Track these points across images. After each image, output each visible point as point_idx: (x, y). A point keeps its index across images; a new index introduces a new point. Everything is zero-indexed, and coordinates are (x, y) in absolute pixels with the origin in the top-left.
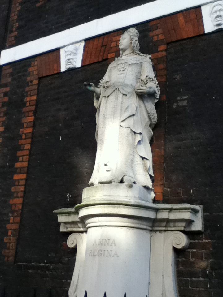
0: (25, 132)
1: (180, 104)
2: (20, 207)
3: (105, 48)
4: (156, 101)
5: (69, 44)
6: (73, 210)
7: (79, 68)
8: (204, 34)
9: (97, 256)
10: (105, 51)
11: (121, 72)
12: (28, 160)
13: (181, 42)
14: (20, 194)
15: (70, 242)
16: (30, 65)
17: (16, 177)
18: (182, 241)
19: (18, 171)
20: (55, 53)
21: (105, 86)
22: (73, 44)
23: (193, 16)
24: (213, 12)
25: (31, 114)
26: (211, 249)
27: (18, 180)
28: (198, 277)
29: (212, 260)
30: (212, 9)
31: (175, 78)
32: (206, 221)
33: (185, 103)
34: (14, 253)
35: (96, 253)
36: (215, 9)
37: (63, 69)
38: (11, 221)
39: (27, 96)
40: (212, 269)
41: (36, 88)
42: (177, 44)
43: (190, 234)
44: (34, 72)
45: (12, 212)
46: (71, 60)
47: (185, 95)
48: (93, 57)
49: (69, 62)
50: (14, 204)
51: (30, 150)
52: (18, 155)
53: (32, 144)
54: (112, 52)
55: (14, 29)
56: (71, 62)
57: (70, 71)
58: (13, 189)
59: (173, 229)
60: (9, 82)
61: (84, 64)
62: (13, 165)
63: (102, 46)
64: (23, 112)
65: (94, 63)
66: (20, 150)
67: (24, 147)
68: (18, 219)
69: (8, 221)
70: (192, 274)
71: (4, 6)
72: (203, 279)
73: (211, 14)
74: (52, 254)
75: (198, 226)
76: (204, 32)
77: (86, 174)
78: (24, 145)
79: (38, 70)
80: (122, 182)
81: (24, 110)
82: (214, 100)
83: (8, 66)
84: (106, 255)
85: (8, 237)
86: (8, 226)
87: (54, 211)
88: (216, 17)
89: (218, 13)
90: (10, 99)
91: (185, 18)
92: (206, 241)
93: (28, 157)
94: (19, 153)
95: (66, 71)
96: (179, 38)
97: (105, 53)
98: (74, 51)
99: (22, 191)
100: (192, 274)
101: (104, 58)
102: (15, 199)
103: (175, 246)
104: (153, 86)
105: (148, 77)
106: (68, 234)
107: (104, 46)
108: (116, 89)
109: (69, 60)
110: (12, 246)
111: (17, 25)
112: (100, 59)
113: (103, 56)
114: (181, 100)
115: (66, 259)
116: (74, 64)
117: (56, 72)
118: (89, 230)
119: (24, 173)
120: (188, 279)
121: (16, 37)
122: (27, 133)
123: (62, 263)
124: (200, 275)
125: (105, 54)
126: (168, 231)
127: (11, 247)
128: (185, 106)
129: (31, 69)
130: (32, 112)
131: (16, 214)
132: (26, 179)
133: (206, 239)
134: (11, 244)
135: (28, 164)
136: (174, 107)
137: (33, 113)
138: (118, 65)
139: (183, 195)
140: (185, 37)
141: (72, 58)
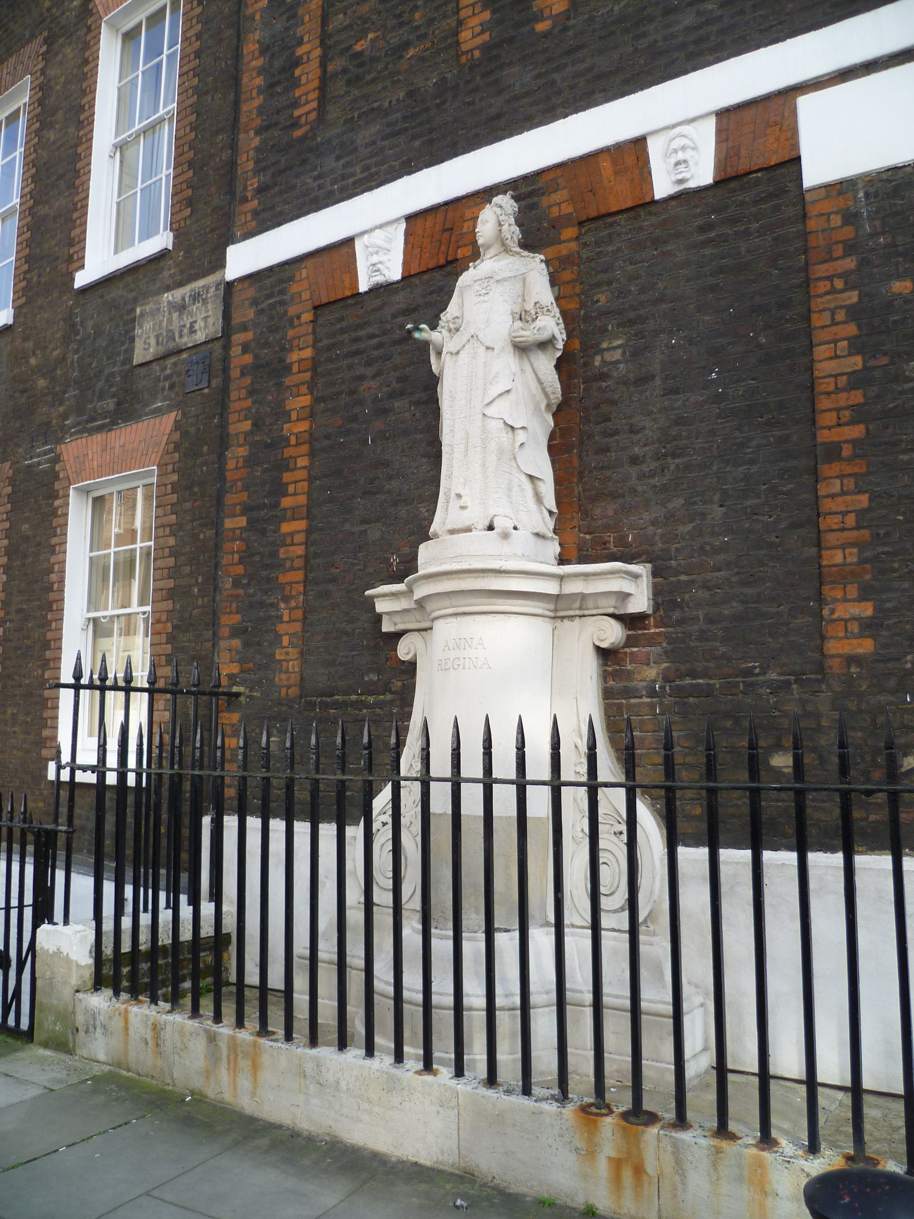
0: (295, 431)
1: (608, 357)
2: (301, 588)
4: (559, 354)
5: (372, 227)
6: (401, 587)
7: (398, 282)
8: (654, 202)
9: (451, 669)
11: (482, 298)
12: (306, 490)
13: (610, 220)
14: (299, 563)
15: (404, 651)
16: (291, 279)
17: (286, 528)
18: (612, 633)
19: (289, 514)
20: (344, 250)
21: (452, 326)
22: (381, 227)
23: (630, 160)
24: (670, 151)
25: (304, 389)
26: (664, 645)
27: (292, 534)
28: (641, 697)
29: (666, 665)
31: (598, 301)
32: (657, 592)
33: (617, 355)
34: (298, 678)
36: (675, 144)
37: (363, 287)
38: (286, 618)
40: (666, 679)
41: (310, 330)
42: (600, 223)
44: (303, 293)
45: (286, 599)
46: (379, 266)
49: (376, 271)
50: (287, 583)
51: (309, 468)
52: (285, 480)
53: (312, 454)
54: (465, 245)
55: (249, 195)
56: (379, 270)
57: (377, 290)
58: (282, 553)
60: (251, 320)
61: (407, 274)
62: (277, 504)
63: (445, 230)
64: (288, 387)
65: (428, 270)
66: (288, 470)
67: (296, 463)
68: (299, 614)
69: (280, 618)
70: (628, 693)
71: (221, 137)
72: (648, 700)
73: (666, 156)
74: (371, 676)
77: (426, 514)
78: (295, 458)
79: (310, 289)
80: (491, 528)
81: (289, 381)
82: (673, 346)
83: (246, 284)
85: (284, 650)
86: (281, 628)
87: (367, 593)
88: (678, 164)
89: (681, 156)
90: (256, 357)
91: (615, 163)
92: (657, 630)
93: (305, 483)
94: (287, 477)
95: (371, 290)
96: (603, 211)
98: (386, 245)
99: (300, 557)
100: (628, 693)
101: (450, 259)
102: (290, 573)
104: (551, 325)
105: (538, 305)
106: (397, 636)
107: (448, 229)
108: (472, 336)
109: (374, 265)
110: (294, 666)
111: (253, 183)
112: (442, 261)
114: (608, 349)
115: (399, 684)
116: (385, 272)
117: (348, 293)
118: (439, 625)
119: (302, 519)
120: (624, 701)
121: (256, 213)
122: (300, 432)
123: (391, 692)
124: (644, 693)
126: (584, 616)
127: (291, 670)
128: (618, 362)
129: (294, 288)
130: (306, 386)
131: (293, 603)
132: (308, 531)
133: (656, 626)
134: (291, 663)
135: (309, 499)
136: (597, 364)
137: (308, 388)
139: (615, 547)
140: (614, 209)
141: (382, 261)
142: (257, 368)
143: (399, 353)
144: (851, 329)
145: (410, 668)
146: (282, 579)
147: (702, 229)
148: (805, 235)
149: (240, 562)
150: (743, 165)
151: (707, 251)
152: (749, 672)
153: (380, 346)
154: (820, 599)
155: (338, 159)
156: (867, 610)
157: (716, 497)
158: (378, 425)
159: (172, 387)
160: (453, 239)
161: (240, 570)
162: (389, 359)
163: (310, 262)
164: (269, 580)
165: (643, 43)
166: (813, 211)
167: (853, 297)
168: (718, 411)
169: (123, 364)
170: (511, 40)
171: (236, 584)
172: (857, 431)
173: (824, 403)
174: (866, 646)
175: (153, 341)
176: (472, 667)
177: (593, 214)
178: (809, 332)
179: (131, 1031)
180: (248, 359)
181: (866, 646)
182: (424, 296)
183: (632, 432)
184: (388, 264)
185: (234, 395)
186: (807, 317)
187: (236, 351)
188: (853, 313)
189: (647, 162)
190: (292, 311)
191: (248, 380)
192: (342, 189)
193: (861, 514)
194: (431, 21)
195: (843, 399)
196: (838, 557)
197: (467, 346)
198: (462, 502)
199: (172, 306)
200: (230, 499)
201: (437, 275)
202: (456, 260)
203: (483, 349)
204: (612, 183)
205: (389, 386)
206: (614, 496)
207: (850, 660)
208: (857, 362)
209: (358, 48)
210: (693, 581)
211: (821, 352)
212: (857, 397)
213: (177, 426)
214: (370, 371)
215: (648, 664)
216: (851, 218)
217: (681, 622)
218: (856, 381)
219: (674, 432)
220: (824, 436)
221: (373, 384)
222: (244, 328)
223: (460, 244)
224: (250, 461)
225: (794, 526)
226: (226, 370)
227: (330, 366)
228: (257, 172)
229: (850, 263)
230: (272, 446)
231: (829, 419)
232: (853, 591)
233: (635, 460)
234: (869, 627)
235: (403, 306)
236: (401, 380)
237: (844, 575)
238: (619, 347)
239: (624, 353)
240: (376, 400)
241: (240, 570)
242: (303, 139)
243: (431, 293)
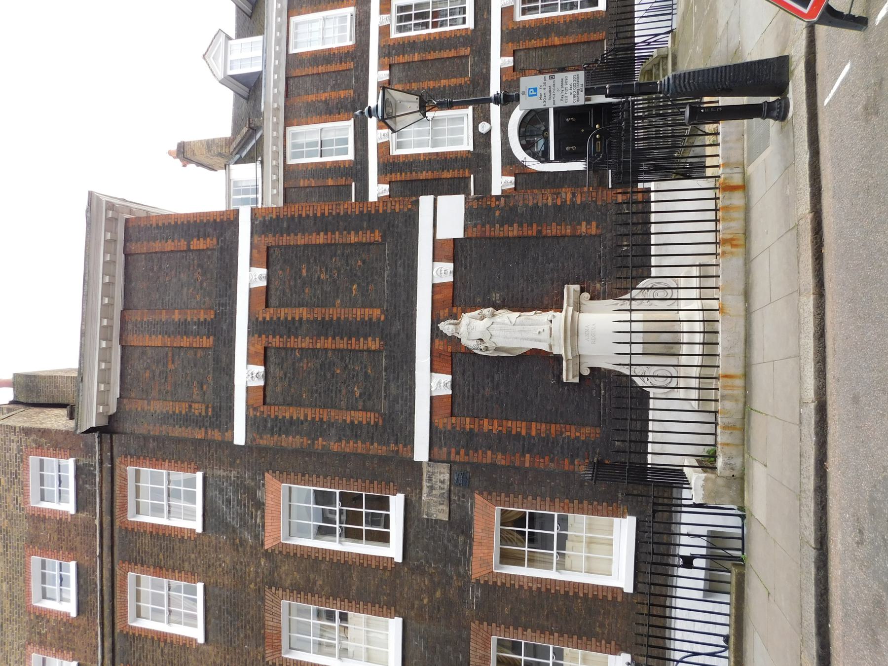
16: (437, 427)
17: (534, 433)
25: (481, 422)
27: (537, 430)
33: (498, 295)
38: (568, 434)
39: (464, 428)
43: (582, 290)
45: (562, 433)
62: (524, 437)
68: (568, 426)
69: (569, 437)
75: (577, 287)
80: (551, 321)
81: (476, 430)
86: (573, 437)
90: (463, 447)
100: (604, 292)
104: (486, 311)
110: (588, 430)
111: (392, 446)
121: (405, 446)
129: (441, 426)
132: (537, 422)
141: (442, 384)
142: (467, 447)
144: (506, 226)
146: (553, 436)
147: (466, 268)
148: (476, 238)
149: (544, 458)
150: (451, 254)
152: (600, 257)
153: (473, 386)
154: (580, 236)
155: (398, 403)
156: (584, 223)
158: (502, 388)
159: (464, 496)
161: (547, 458)
163: (434, 418)
164: (553, 443)
165: (402, 283)
166: (470, 235)
167: (497, 226)
169: (445, 529)
170: (383, 329)
171: (552, 461)
172: (535, 226)
173: (525, 234)
174: (594, 224)
175: (441, 507)
178: (504, 238)
179: (729, 442)
180: (462, 452)
181: (594, 224)
185: (475, 461)
186: (499, 238)
187: (458, 458)
188: (502, 226)
190: (449, 428)
191: (471, 452)
192: (410, 401)
193: (557, 225)
194: (362, 363)
195: (525, 229)
196: (569, 231)
199: (429, 494)
200: (517, 464)
201: (454, 361)
206: (542, 297)
207: (597, 227)
208: (515, 225)
209: (358, 395)
211: (511, 234)
212: (525, 225)
213: (481, 494)
214: (482, 391)
216: (475, 226)
217: (583, 276)
218: (521, 225)
220: (534, 234)
221: (487, 390)
222: (449, 453)
224: (504, 452)
225: (558, 243)
226: (464, 463)
227: (475, 410)
228: (388, 445)
229: (488, 226)
230: (500, 439)
231: (530, 233)
232: (579, 227)
233: (532, 290)
234: (589, 223)
237: (574, 229)
240: (493, 389)
241: (547, 458)
242: (384, 420)
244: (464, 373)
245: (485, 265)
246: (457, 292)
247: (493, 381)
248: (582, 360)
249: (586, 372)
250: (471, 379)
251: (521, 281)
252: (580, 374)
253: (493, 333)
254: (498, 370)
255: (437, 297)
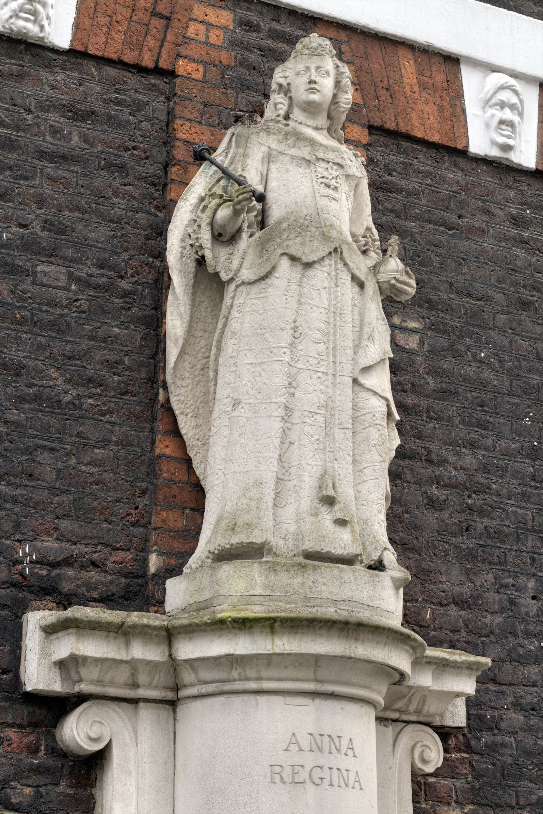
3: (167, 27)
8: (464, 153)
9: (309, 786)
10: (164, 40)
11: (330, 192)
24: (494, 101)
30: (496, 92)
35: (304, 775)
36: (506, 96)
47: (412, 319)
48: (119, 38)
54: (193, 60)
56: (35, 13)
59: (414, 718)
61: (81, 48)
63: (155, 14)
65: (119, 63)
73: (487, 103)
75: (457, 716)
76: (467, 146)
82: (481, 362)
84: (335, 783)
88: (502, 122)
89: (507, 114)
97: (166, 44)
101: (163, 64)
103: (419, 765)
108: (335, 250)
112: (148, 61)
113: (159, 54)
116: (45, 22)
125: (164, 51)
138: (318, 159)
140: (419, 134)
143: (50, 178)
145: (91, 766)
147: (515, 221)
151: (520, 253)
157: (531, 584)
160: (170, 37)
162: (27, 179)
168: (532, 469)
176: (343, 785)
177: (391, 125)
182: (105, 101)
183: (430, 461)
184: (51, 12)
189: (460, 95)
197: (327, 262)
198: (338, 512)
201: (133, 80)
202: (171, 74)
203: (348, 278)
204: (416, 96)
205: (25, 226)
210: (503, 693)
215: (449, 804)
217: (493, 748)
219: (481, 479)
223: (183, 50)
233: (433, 504)
235: (65, 98)
236: (47, 225)
238: (414, 331)
239: (421, 343)
243: (119, 103)
244: (78, 114)
245: (526, 305)
246: (423, 161)
247: (29, 246)
248: (146, 713)
249: (78, 731)
250: (48, 143)
251: (469, 459)
252: (81, 699)
253: (320, 275)
254: (85, 283)
255: (408, 67)
